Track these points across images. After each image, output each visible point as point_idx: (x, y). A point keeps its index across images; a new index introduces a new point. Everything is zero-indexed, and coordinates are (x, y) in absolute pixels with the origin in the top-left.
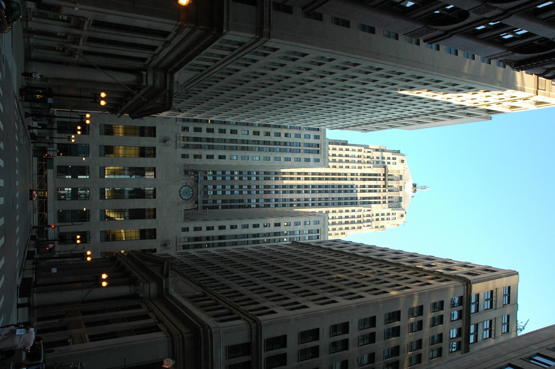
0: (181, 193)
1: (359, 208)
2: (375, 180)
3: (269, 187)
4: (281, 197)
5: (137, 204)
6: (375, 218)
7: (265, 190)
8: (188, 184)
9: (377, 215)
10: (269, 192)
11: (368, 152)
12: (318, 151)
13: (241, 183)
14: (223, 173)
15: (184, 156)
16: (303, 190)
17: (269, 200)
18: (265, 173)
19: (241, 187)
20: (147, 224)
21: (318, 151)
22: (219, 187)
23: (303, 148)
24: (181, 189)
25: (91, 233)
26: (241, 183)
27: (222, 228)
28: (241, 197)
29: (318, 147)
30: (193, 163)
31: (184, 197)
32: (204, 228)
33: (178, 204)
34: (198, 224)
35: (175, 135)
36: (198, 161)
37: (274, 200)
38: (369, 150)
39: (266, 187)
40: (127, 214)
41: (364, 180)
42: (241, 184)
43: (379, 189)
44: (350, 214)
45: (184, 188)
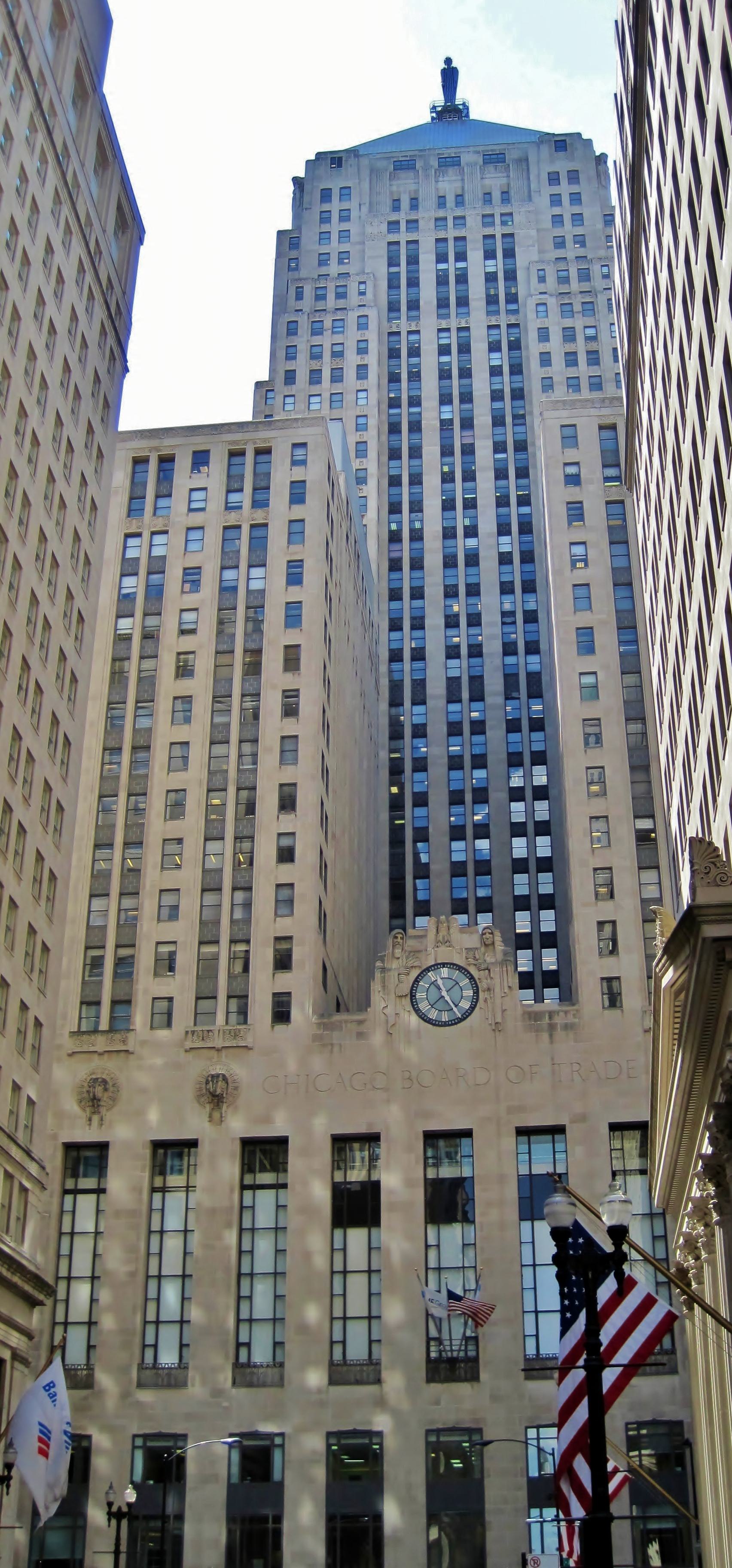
0: (445, 1017)
1: (531, 315)
2: (413, 260)
3: (453, 683)
4: (498, 630)
6: (572, 251)
7: (465, 695)
8: (406, 989)
9: (560, 243)
10: (477, 681)
11: (299, 296)
12: (258, 452)
13: (438, 798)
16: (463, 544)
17: (510, 680)
21: (258, 452)
23: (247, 516)
24: (429, 1021)
25: (632, 1418)
29: (242, 453)
31: (466, 1005)
33: (497, 1027)
35: (190, 1055)
36: (304, 954)
38: (292, 293)
39: (453, 697)
41: (414, 305)
42: (445, 798)
43: (451, 243)
44: (556, 346)
45: (424, 1006)
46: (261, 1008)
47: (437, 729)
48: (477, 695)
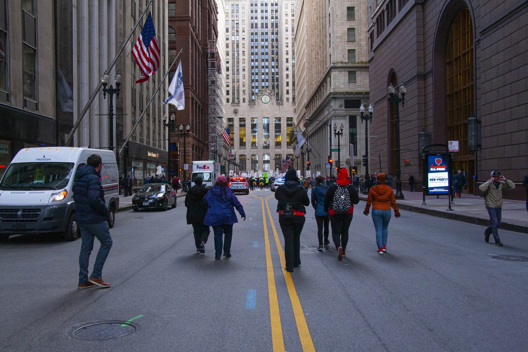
3: (262, 24)
5: (272, 128)
13: (260, 47)
14: (252, 61)
15: (244, 101)
17: (272, 24)
18: (252, 27)
19: (263, 47)
20: (284, 123)
22: (263, 71)
26: (260, 47)
27: (287, 76)
28: (270, 40)
30: (248, 95)
32: (288, 88)
34: (285, 92)
37: (273, 20)
39: (262, 27)
40: (278, 134)
46: (241, 101)
47: (259, 34)
48: (267, 27)
